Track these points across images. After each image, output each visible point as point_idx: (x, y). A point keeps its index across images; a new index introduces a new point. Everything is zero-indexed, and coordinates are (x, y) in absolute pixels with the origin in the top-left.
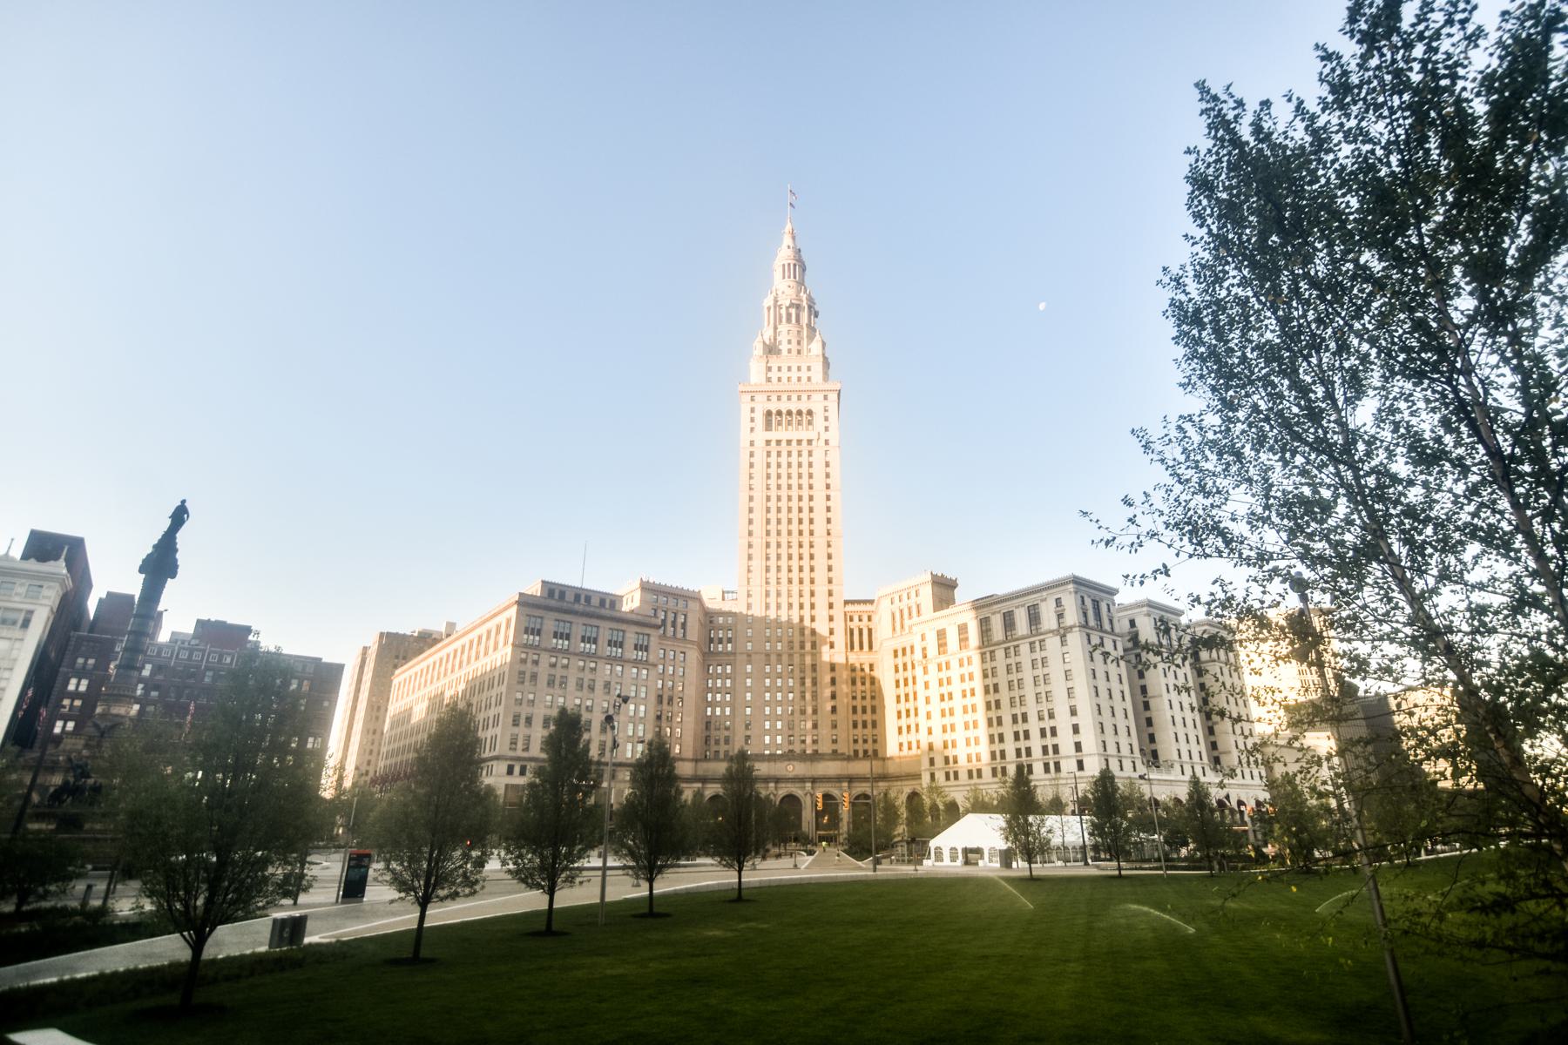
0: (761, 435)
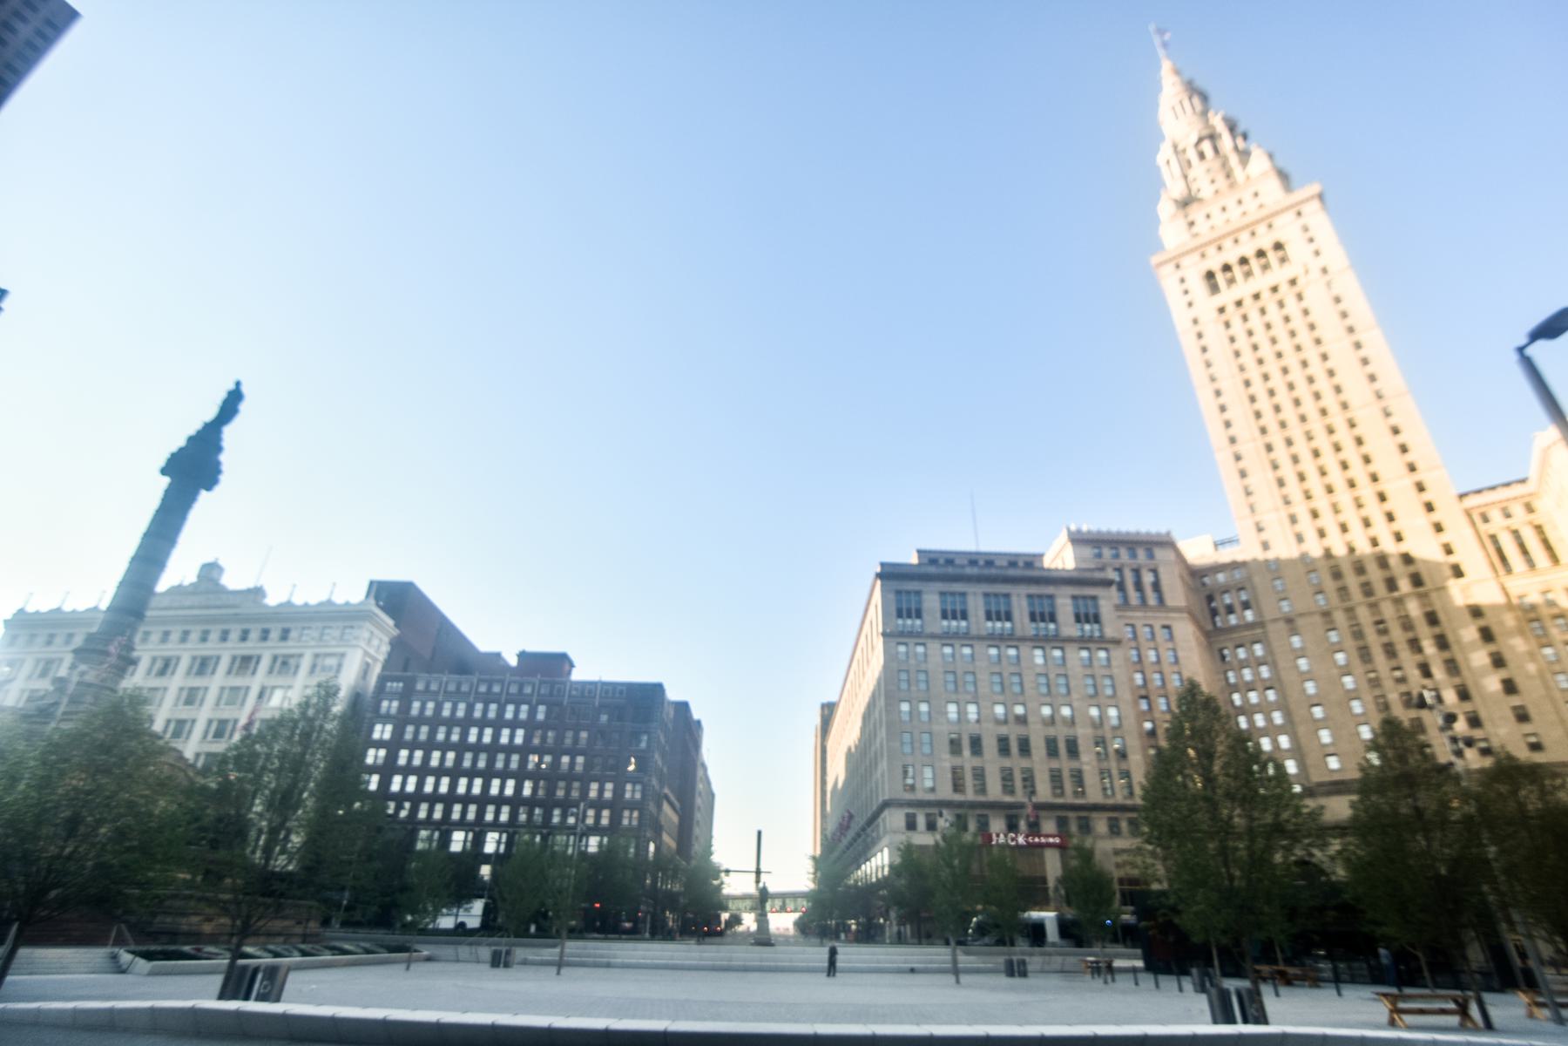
0: (1206, 304)
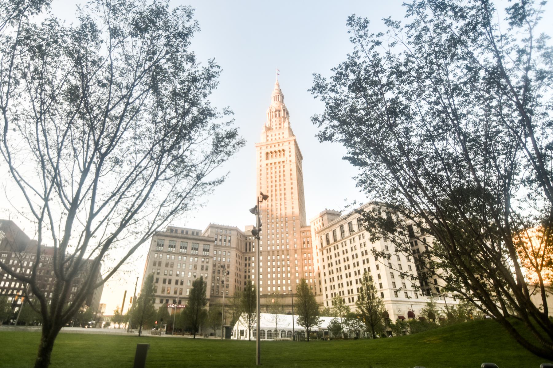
0: (264, 162)
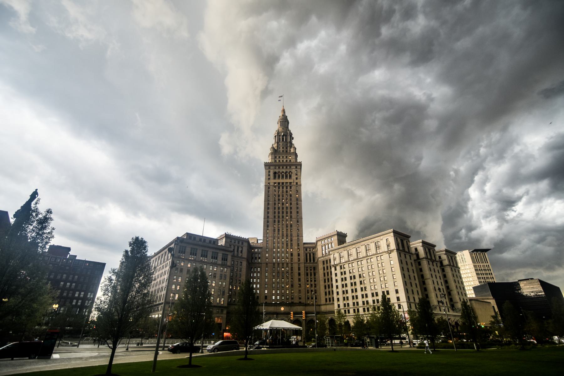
0: (272, 181)
